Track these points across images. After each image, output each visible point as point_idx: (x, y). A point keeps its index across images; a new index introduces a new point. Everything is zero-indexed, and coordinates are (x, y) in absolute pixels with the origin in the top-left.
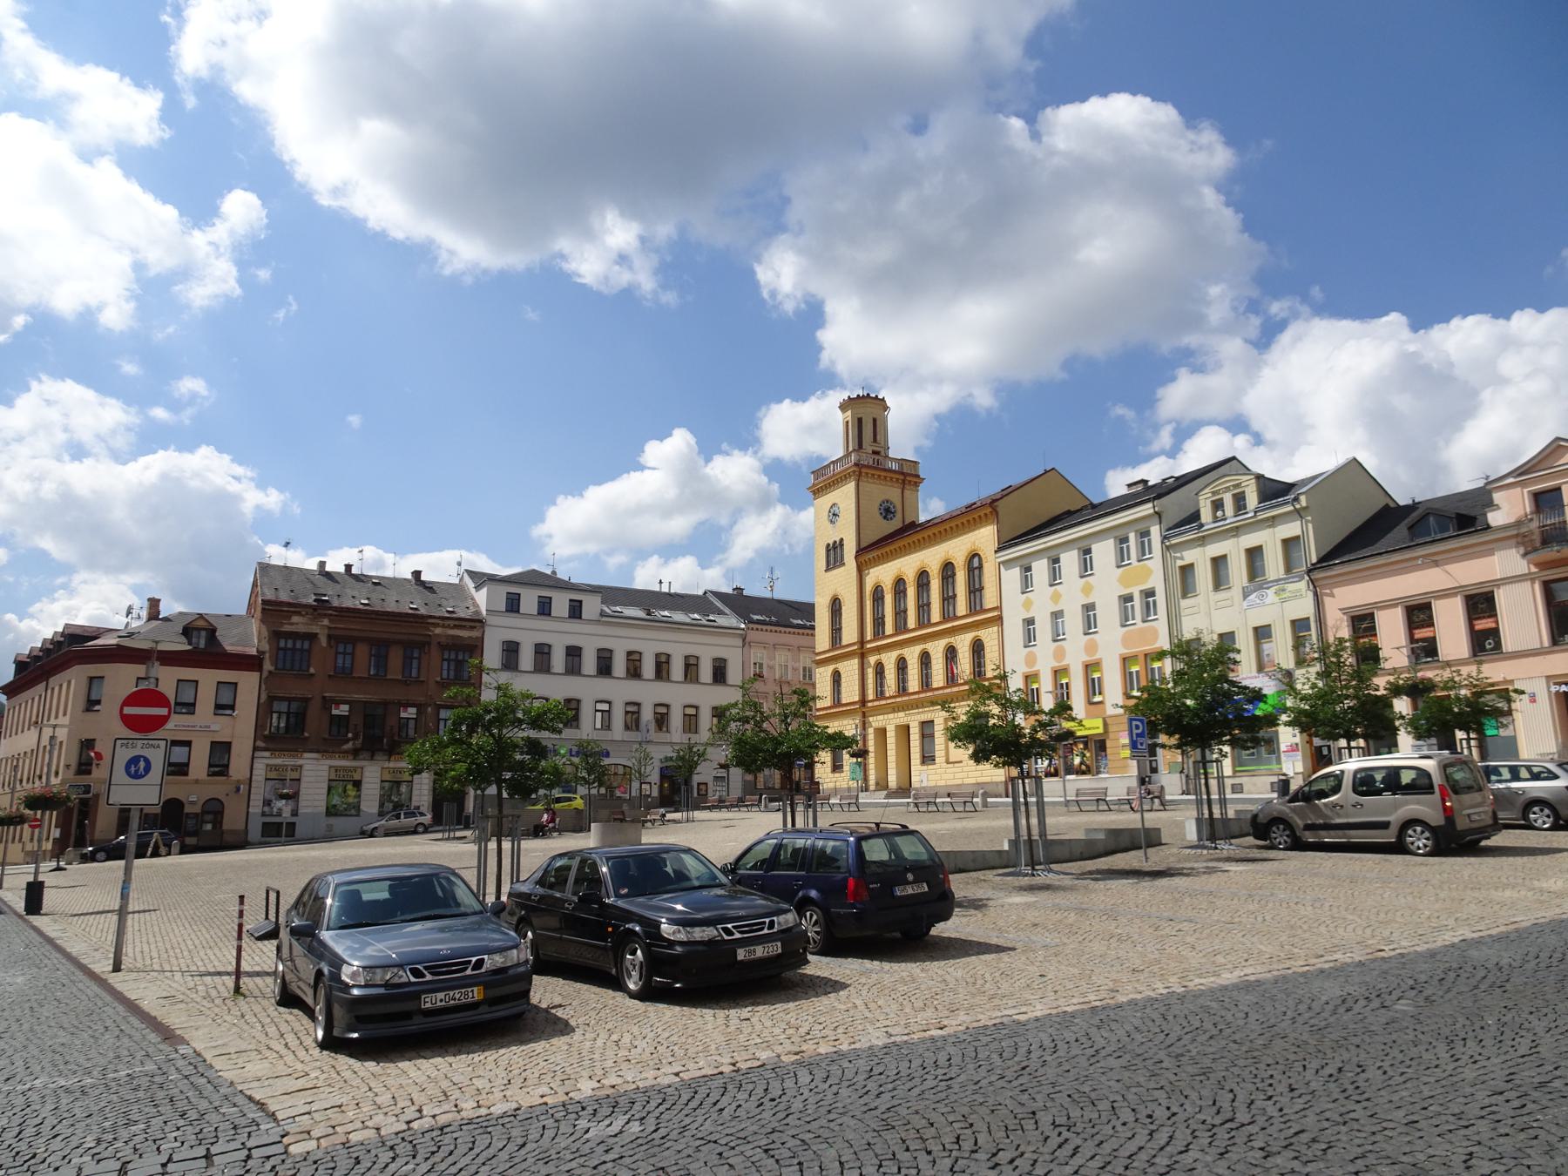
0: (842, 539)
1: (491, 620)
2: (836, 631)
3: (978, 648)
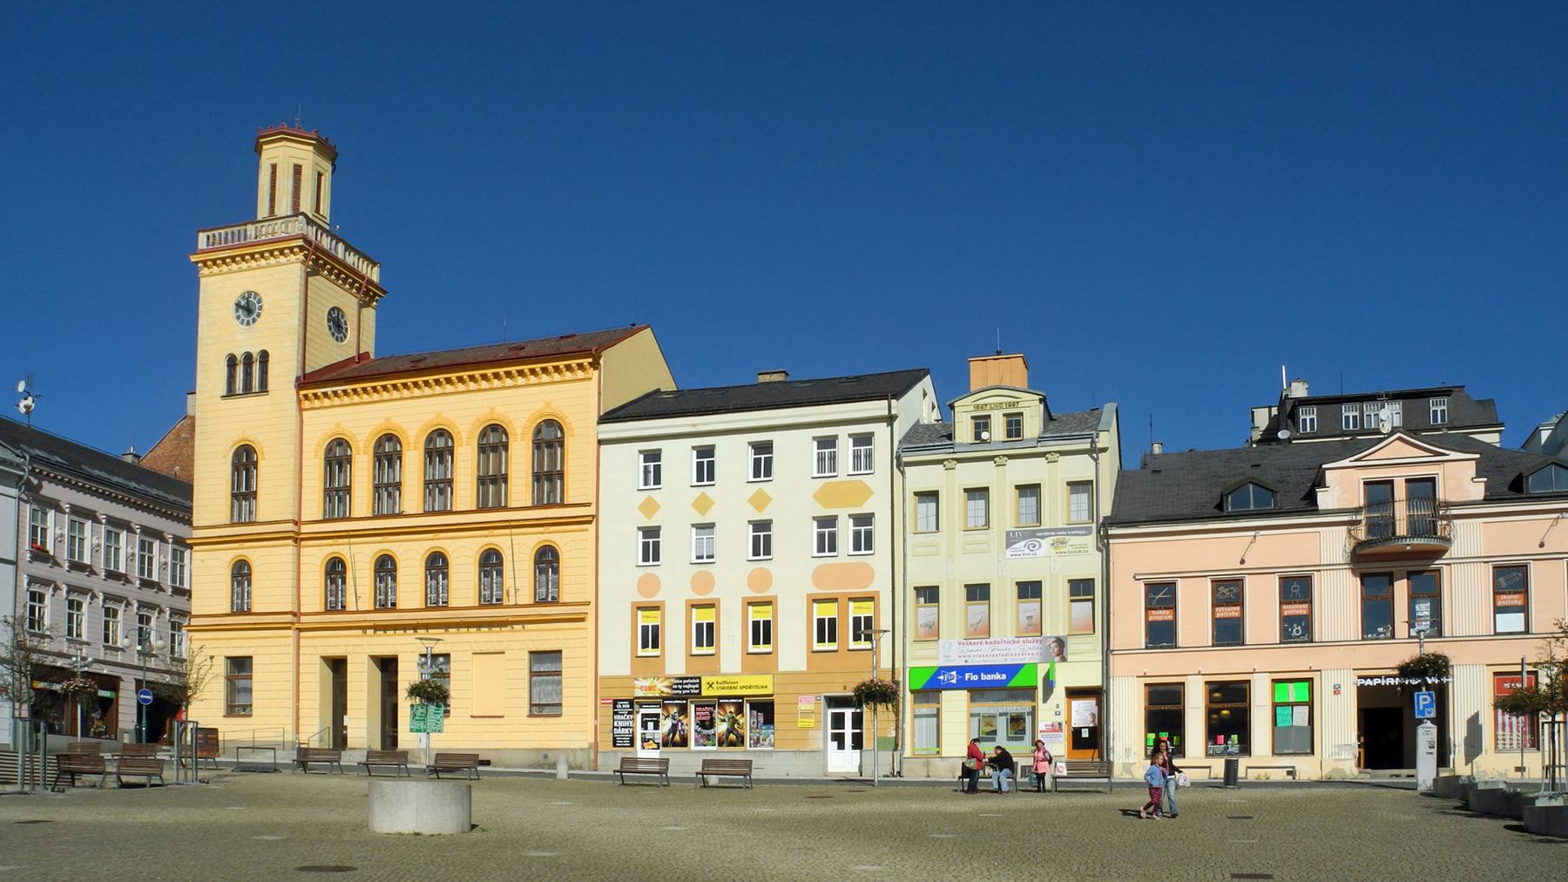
3: (547, 559)
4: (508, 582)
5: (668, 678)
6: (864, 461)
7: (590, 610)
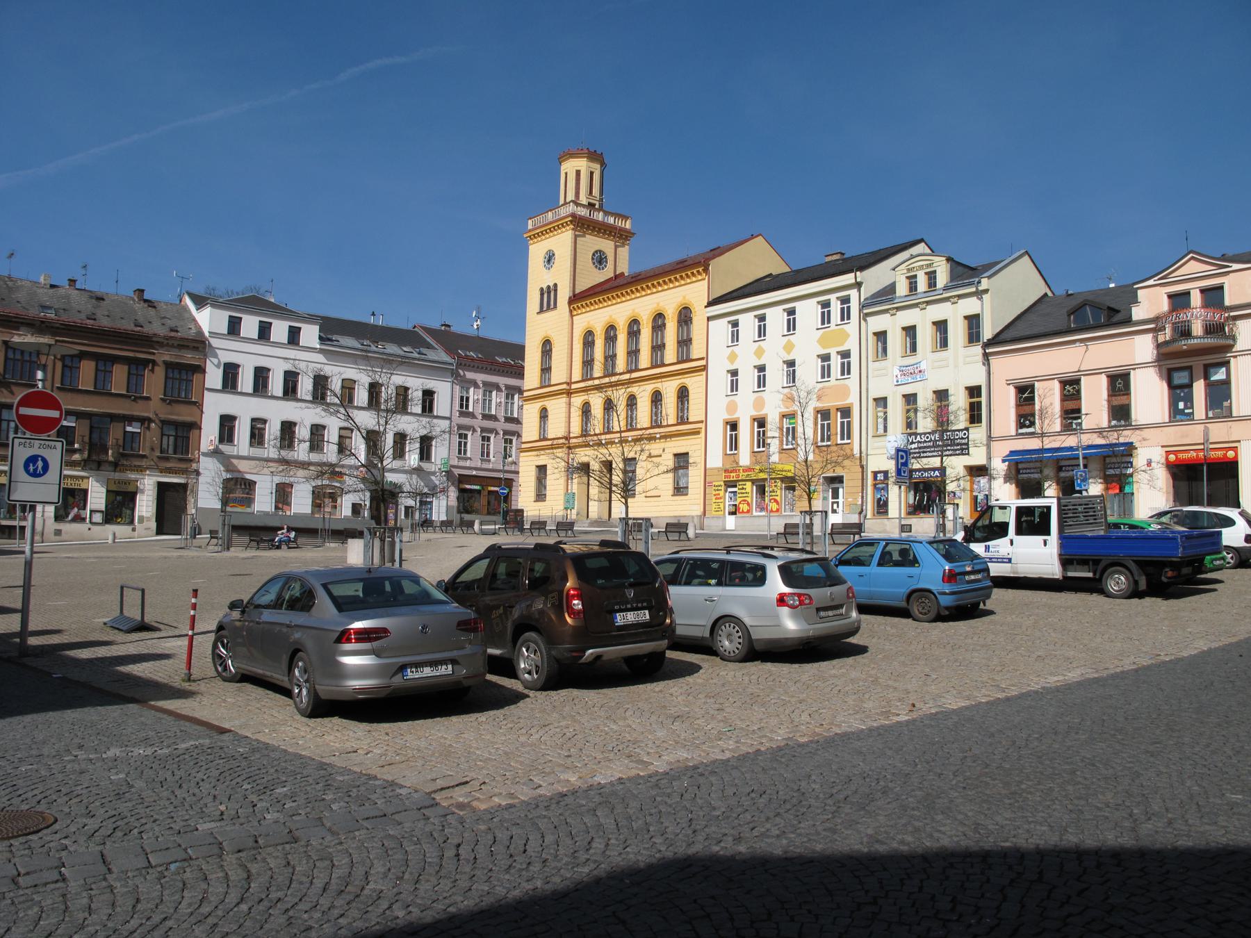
1: (215, 342)
2: (546, 370)
3: (683, 394)
6: (845, 315)
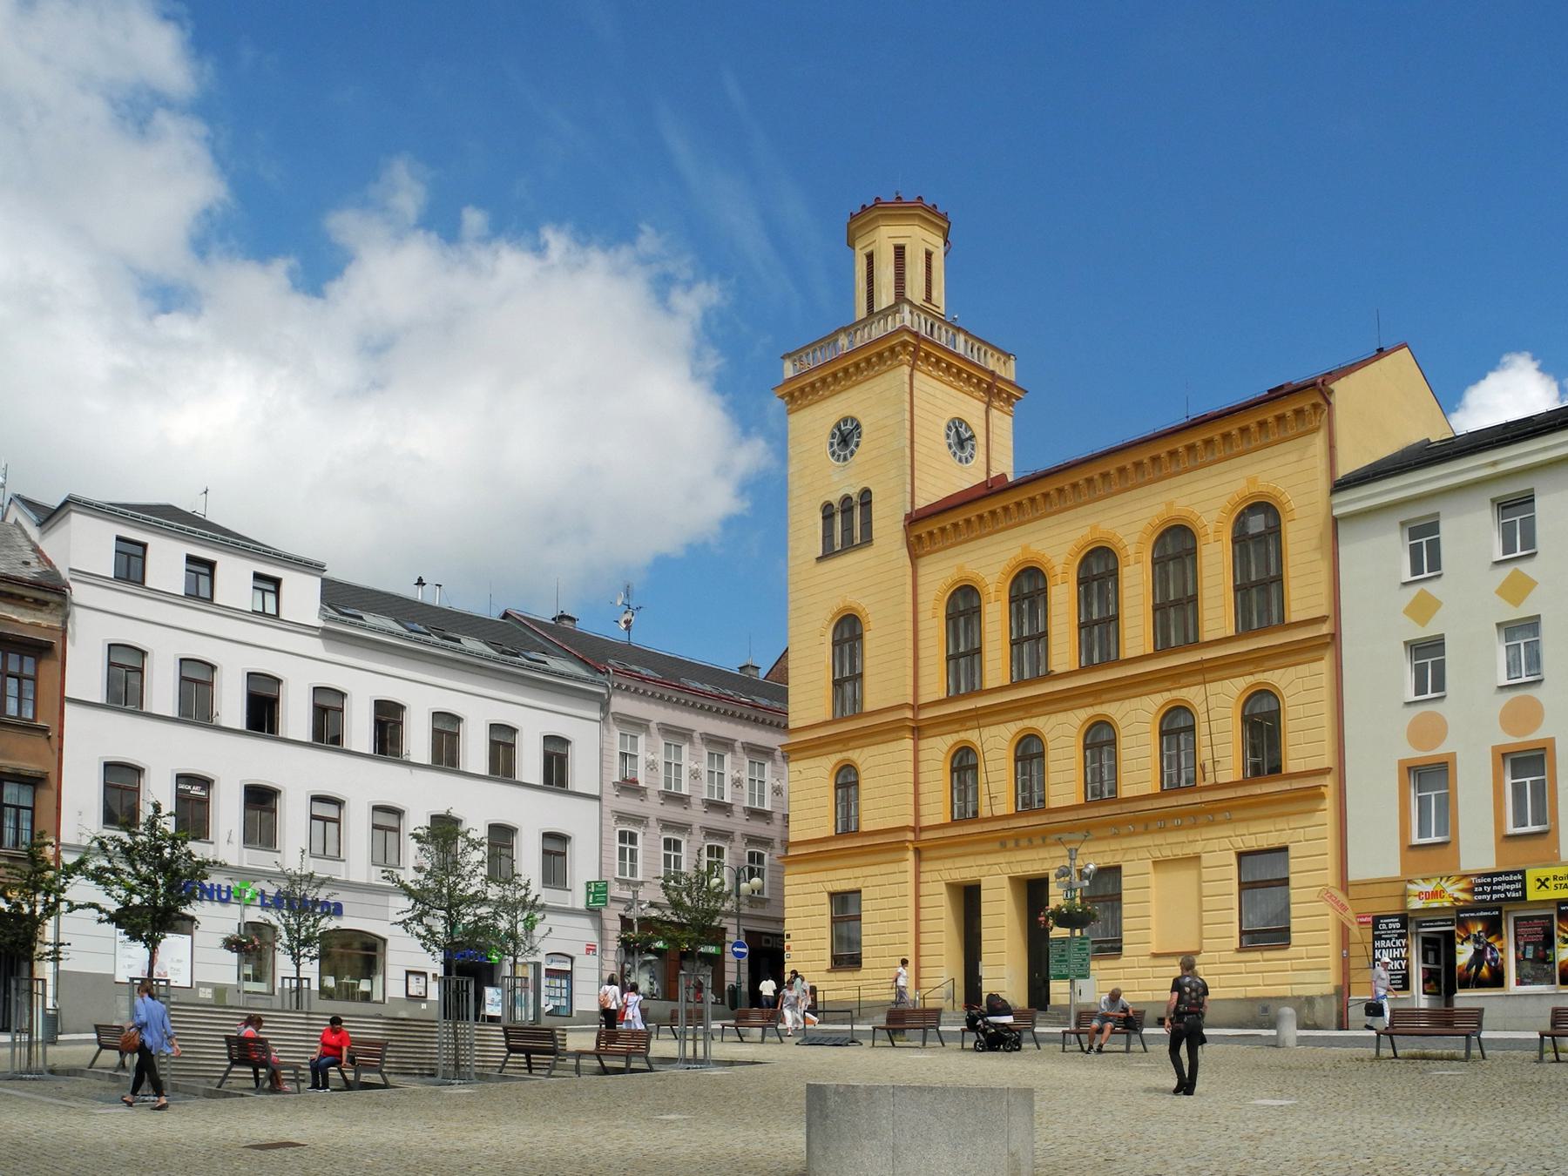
0: (866, 494)
2: (847, 681)
4: (1204, 754)
5: (1466, 876)
7: (1329, 781)
